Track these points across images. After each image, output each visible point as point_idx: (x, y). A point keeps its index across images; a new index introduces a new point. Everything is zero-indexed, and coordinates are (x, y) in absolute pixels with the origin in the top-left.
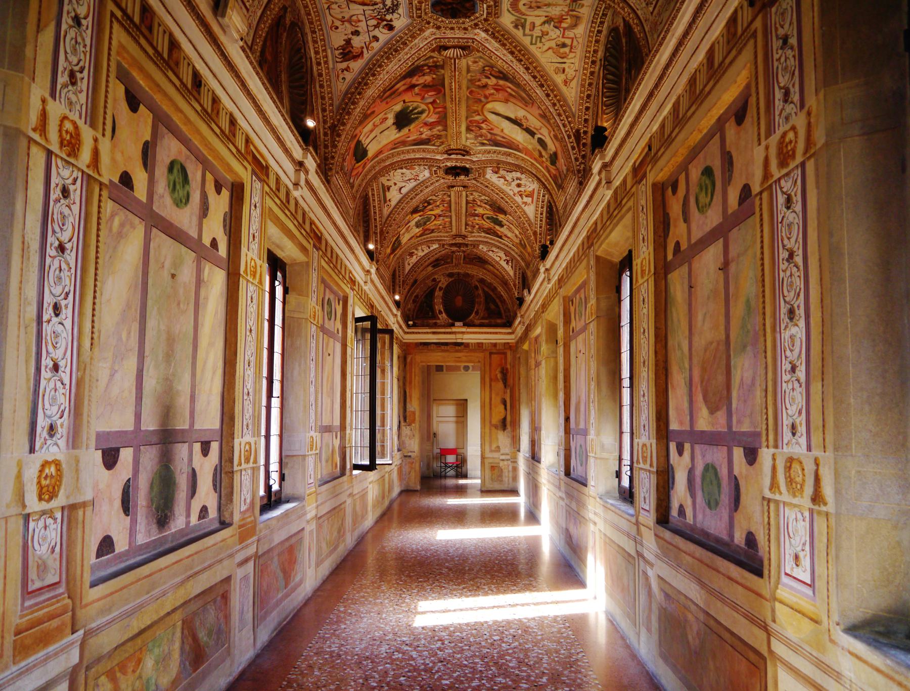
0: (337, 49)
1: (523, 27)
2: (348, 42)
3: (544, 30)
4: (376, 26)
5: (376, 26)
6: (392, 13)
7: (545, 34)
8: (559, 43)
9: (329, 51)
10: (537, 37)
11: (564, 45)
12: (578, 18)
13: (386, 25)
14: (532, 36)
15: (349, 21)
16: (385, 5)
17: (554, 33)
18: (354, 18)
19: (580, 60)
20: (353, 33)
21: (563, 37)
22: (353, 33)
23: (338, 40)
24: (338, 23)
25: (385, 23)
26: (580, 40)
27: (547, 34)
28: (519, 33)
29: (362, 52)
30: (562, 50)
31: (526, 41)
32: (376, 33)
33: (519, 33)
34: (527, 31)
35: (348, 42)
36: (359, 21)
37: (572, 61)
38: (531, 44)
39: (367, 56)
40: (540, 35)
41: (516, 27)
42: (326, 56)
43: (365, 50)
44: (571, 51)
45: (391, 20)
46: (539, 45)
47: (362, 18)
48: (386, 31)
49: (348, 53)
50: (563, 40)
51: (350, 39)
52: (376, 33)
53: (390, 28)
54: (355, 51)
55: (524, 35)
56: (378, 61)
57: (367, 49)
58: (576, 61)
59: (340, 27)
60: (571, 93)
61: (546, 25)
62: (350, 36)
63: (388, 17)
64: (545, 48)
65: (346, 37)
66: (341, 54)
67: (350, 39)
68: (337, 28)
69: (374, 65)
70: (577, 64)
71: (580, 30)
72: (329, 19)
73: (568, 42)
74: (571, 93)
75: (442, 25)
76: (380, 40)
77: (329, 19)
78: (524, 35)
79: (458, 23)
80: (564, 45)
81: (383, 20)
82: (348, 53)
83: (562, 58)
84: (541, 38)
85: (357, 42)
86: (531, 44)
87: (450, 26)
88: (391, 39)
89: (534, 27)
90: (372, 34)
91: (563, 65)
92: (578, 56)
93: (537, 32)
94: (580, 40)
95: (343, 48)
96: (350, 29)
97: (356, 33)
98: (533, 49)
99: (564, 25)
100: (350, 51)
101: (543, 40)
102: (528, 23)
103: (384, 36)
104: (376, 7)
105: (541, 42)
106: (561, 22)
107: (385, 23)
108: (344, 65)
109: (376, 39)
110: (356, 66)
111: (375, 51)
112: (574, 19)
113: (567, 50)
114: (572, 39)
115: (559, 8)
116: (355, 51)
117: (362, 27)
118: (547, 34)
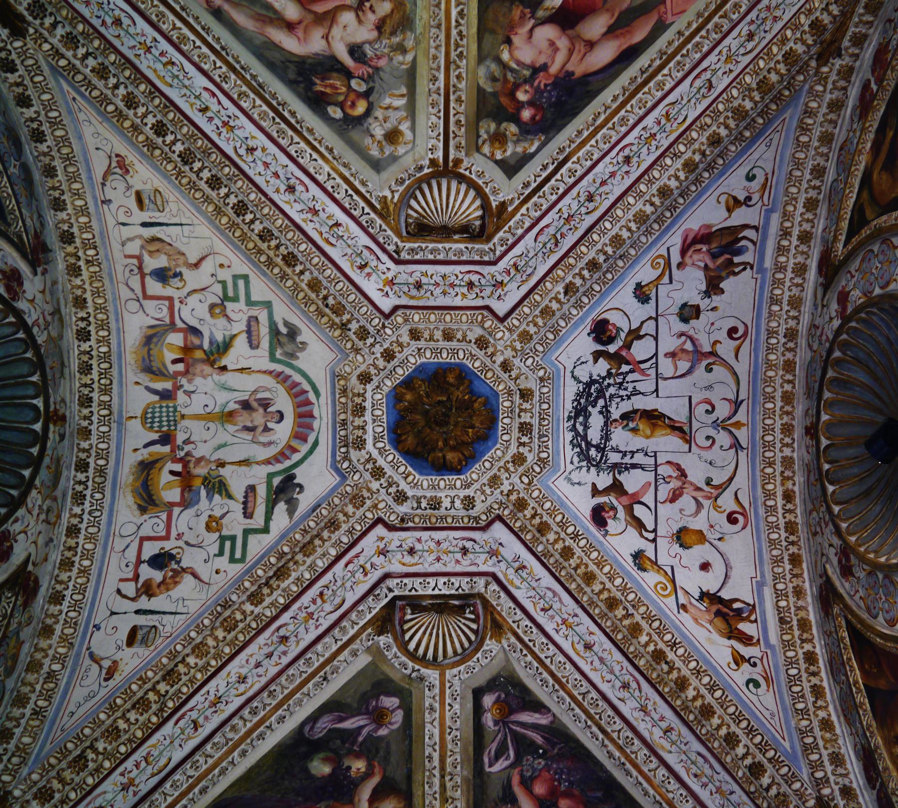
0: (746, 265)
1: (274, 332)
2: (713, 287)
3: (222, 321)
4: (635, 335)
5: (635, 335)
6: (592, 382)
7: (218, 309)
8: (176, 282)
9: (768, 263)
10: (235, 299)
11: (162, 275)
12: (150, 369)
13: (611, 340)
14: (250, 303)
15: (698, 355)
16: (605, 412)
17: (194, 311)
18: (684, 366)
19: (104, 234)
20: (696, 312)
21: (170, 299)
22: (696, 312)
23: (739, 289)
24: (726, 349)
25: (612, 348)
26: (125, 293)
27: (212, 307)
28: (283, 312)
29: (683, 252)
30: (161, 261)
31: (261, 289)
32: (639, 312)
33: (283, 312)
34: (263, 317)
35: (713, 287)
36: (672, 355)
37: (126, 232)
38: (246, 277)
39: (675, 240)
40: (230, 306)
41: (293, 332)
42: (781, 250)
43: (676, 258)
44: (139, 258)
45: (597, 355)
46: (225, 275)
47: (666, 367)
48: (615, 318)
49: (721, 251)
50: (168, 291)
51: (707, 294)
52: (639, 312)
53: (601, 331)
54: (700, 257)
55: (268, 305)
56: (648, 233)
57: (668, 263)
58: (116, 234)
59: (722, 335)
60: (96, 139)
61: (219, 338)
62: (704, 304)
63: (603, 366)
64: (208, 266)
65: (716, 300)
66: (740, 252)
67: (707, 294)
68: (732, 331)
69: (659, 220)
70: (111, 222)
71: (134, 325)
72: (742, 368)
73: (154, 287)
74: (96, 139)
75: (475, 350)
76: (631, 287)
77: (742, 368)
78: (268, 305)
79: (437, 352)
80: (162, 275)
81: (617, 359)
82: (721, 251)
83: (154, 239)
84: (225, 298)
85: (690, 284)
86: (246, 277)
87: (454, 344)
88: (603, 295)
89: (249, 332)
90: (649, 309)
91: (146, 216)
92: (116, 246)
93: (238, 311)
94: (125, 293)
95: (729, 268)
96: (697, 327)
97: (689, 313)
98: (241, 266)
99: (176, 339)
100: (714, 256)
101: (218, 288)
102: (265, 343)
103: (621, 307)
104: (626, 407)
105: (223, 283)
106: (187, 349)
107: (612, 348)
108: (740, 216)
109: (641, 294)
110: (708, 214)
111: (653, 253)
112: (156, 365)
113: (152, 263)
114: (146, 297)
115: (196, 405)
116: (700, 257)
117: (671, 325)
118: (212, 307)
